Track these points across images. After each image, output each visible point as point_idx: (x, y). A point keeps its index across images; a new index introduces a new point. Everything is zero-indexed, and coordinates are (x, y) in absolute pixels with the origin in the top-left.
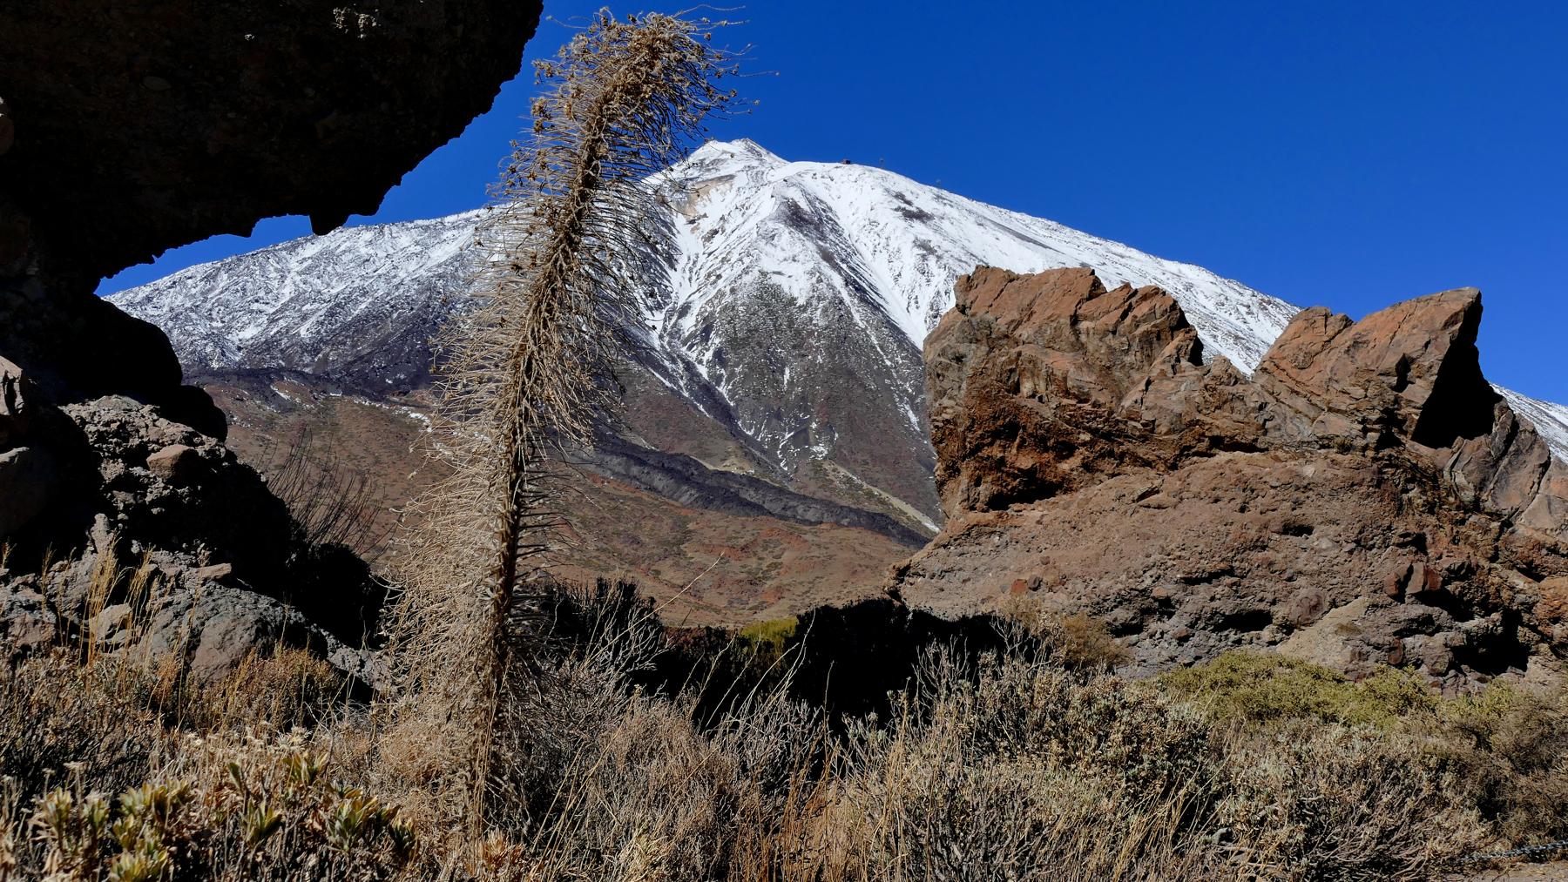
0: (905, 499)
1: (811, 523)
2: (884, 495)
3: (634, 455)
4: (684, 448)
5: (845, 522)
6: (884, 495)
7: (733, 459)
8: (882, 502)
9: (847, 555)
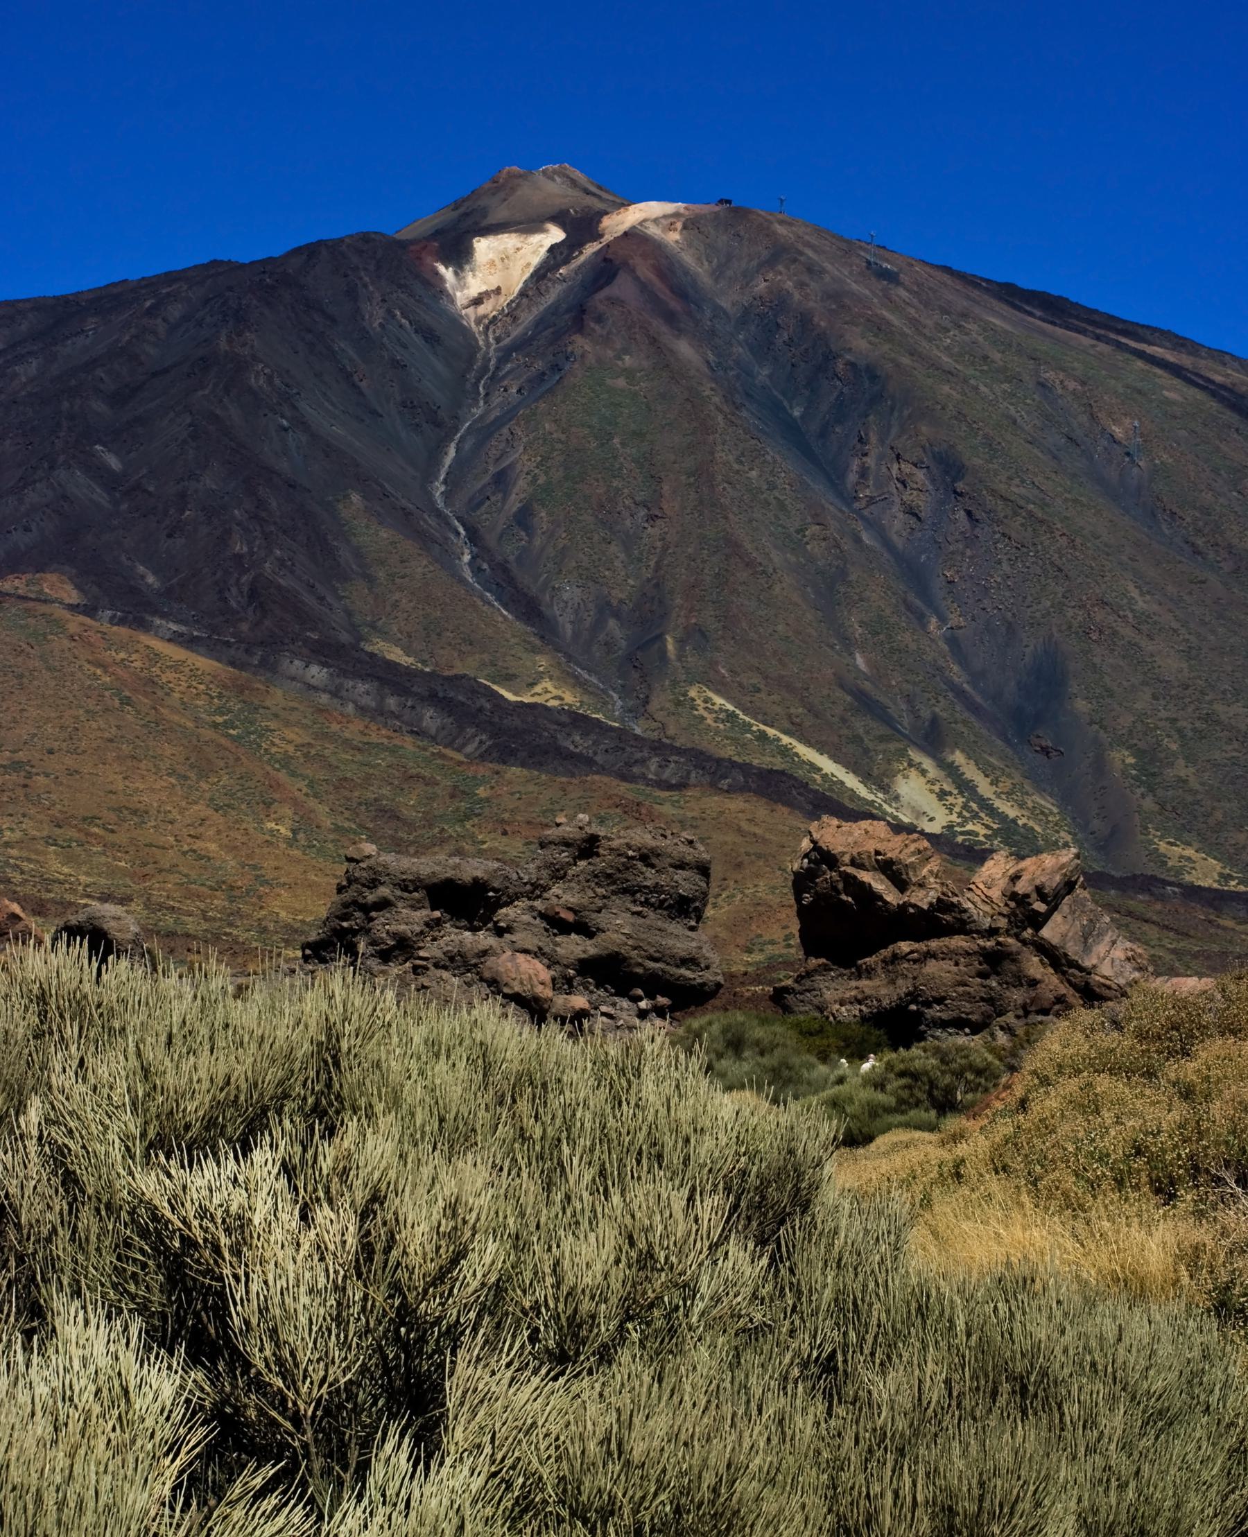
0: (821, 748)
3: (389, 677)
4: (465, 667)
5: (724, 784)
6: (786, 740)
7: (547, 684)
8: (785, 752)
9: (731, 838)
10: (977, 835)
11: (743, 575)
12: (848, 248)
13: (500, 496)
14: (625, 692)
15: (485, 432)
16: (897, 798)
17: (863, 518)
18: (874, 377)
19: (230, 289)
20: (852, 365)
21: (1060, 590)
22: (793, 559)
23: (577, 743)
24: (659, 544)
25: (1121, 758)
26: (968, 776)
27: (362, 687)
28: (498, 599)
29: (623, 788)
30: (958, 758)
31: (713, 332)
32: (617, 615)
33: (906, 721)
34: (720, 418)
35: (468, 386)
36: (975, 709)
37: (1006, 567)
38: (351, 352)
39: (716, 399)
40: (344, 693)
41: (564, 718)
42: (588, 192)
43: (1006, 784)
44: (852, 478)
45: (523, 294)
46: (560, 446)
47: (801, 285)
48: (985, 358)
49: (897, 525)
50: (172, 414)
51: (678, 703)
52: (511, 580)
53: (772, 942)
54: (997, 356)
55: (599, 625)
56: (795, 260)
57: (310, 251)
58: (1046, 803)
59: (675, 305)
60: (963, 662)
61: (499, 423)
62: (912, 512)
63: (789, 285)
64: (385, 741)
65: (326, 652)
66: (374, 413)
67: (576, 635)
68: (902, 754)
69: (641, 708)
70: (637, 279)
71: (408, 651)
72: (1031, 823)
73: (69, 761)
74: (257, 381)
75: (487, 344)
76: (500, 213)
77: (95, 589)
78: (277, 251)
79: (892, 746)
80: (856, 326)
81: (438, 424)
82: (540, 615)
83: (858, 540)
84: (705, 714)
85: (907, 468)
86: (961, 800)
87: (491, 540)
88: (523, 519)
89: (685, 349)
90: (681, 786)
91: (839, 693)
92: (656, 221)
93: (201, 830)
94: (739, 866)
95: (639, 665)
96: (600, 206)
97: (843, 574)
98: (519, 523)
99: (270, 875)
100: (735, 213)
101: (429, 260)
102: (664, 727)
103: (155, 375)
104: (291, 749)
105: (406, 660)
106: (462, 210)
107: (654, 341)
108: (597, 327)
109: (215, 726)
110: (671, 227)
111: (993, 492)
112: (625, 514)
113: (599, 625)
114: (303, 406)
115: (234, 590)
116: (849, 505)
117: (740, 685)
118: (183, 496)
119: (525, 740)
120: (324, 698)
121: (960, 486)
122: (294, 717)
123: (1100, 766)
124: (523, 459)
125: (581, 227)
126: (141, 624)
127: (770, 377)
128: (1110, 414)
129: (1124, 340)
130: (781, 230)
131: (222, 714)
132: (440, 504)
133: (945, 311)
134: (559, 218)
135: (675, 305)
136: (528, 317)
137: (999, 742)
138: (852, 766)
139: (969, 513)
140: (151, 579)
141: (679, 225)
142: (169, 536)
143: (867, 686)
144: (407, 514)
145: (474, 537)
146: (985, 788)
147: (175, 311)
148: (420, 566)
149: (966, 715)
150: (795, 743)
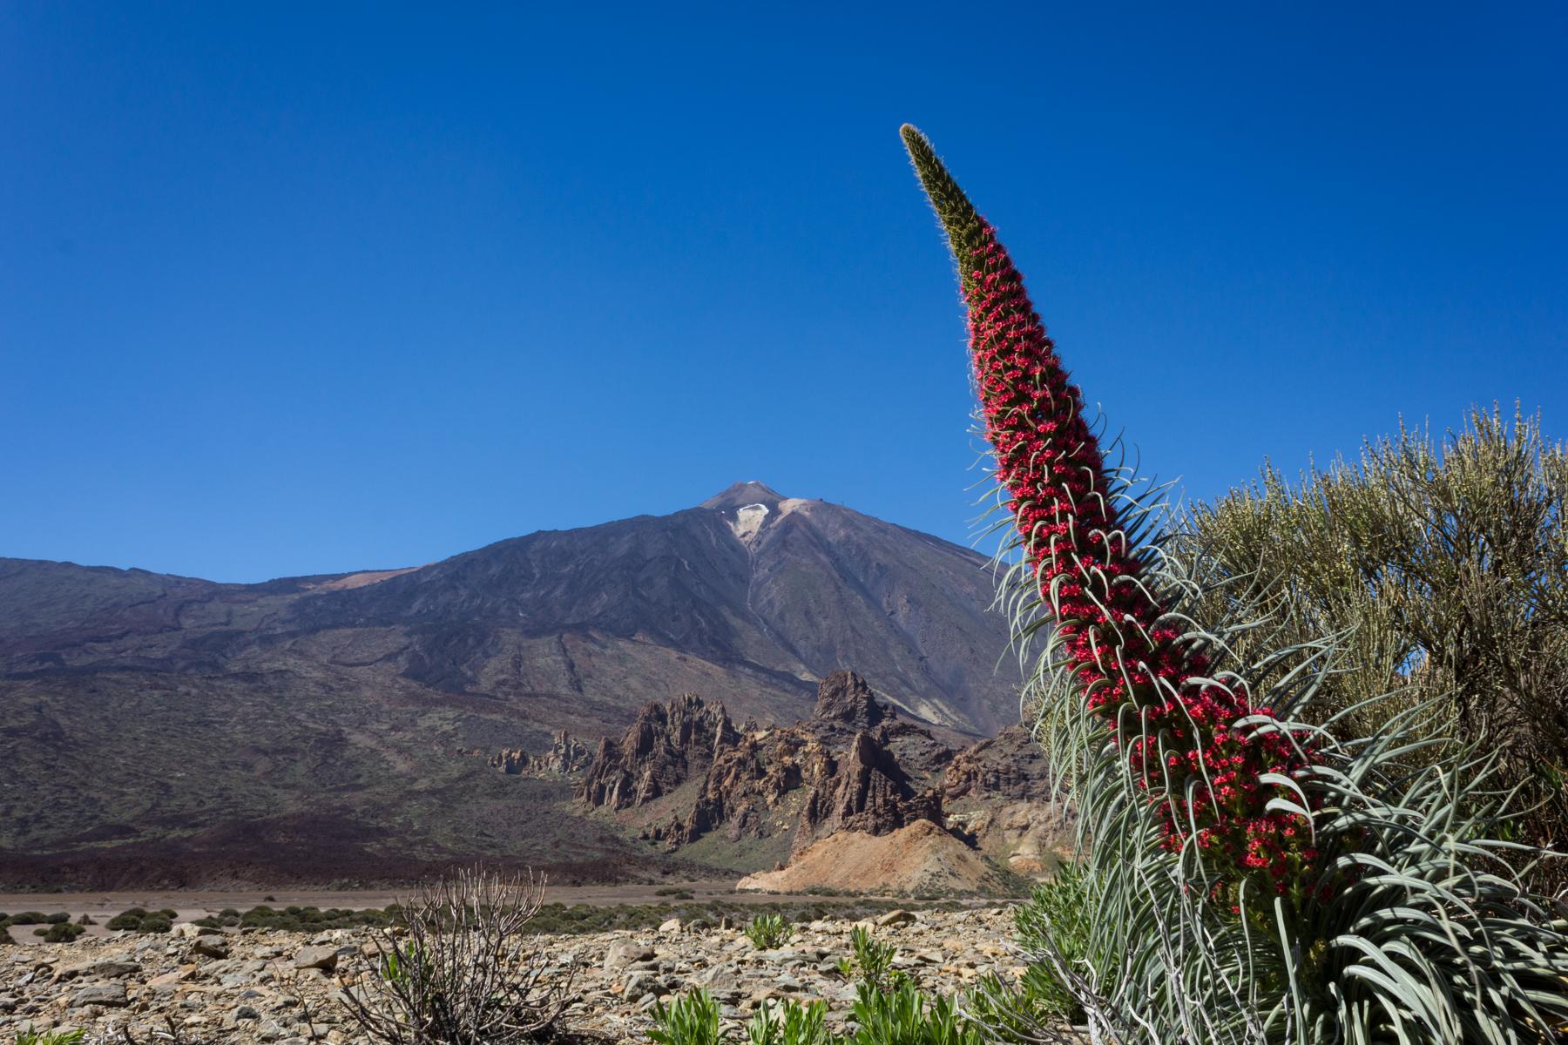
12: (869, 519)
15: (759, 584)
25: (986, 702)
76: (740, 501)
88: (781, 616)
89: (823, 557)
123: (980, 704)
136: (764, 542)
145: (766, 622)
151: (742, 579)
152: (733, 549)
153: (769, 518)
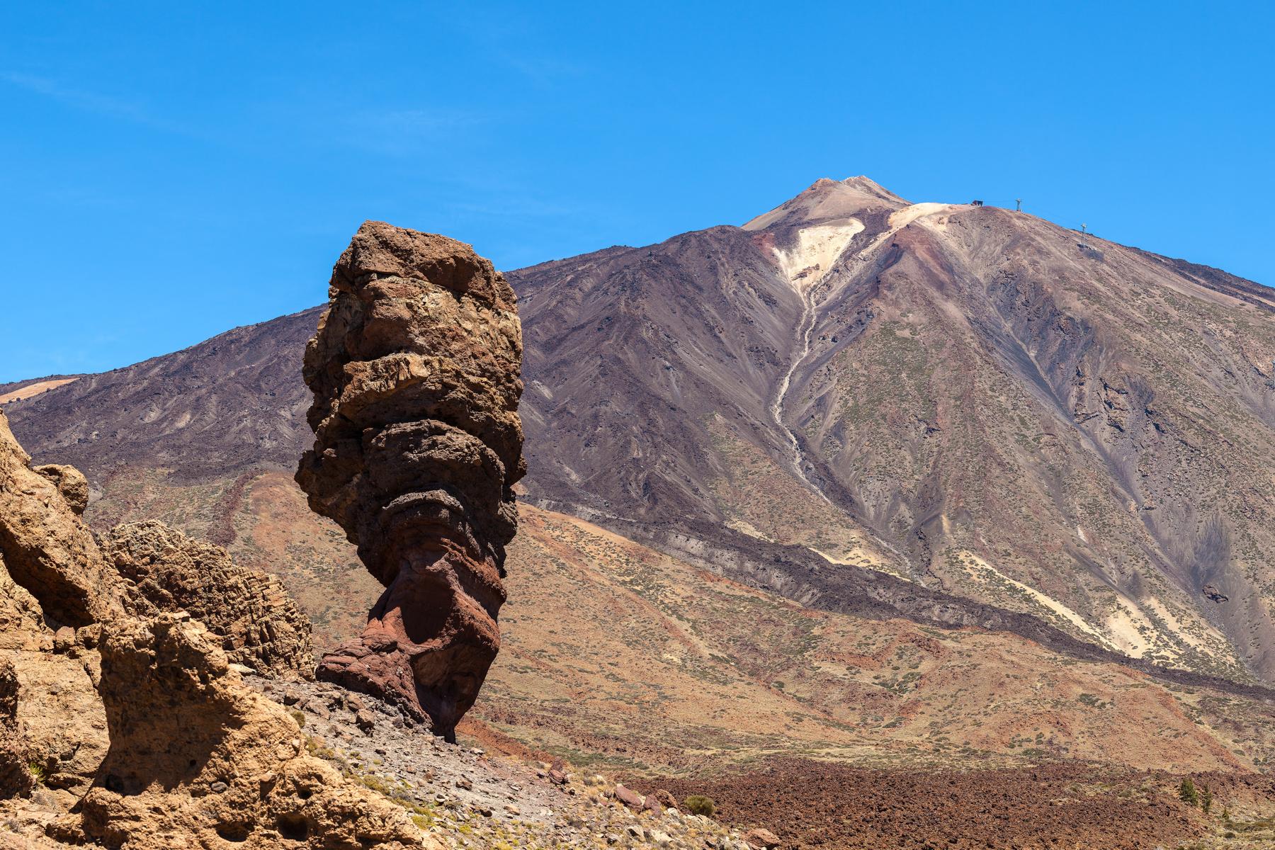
0: (1054, 595)
1: (949, 627)
2: (1029, 591)
3: (744, 546)
4: (801, 538)
5: (988, 624)
6: (1029, 591)
8: (1028, 599)
10: (1168, 658)
11: (997, 471)
13: (821, 415)
14: (912, 555)
15: (809, 369)
16: (1110, 632)
17: (1081, 429)
18: (1087, 328)
19: (627, 267)
20: (1070, 318)
21: (1223, 481)
22: (1032, 460)
23: (880, 594)
24: (935, 449)
26: (1160, 616)
27: (727, 555)
28: (822, 490)
29: (916, 629)
30: (1153, 602)
31: (971, 297)
32: (906, 500)
33: (1115, 576)
34: (978, 358)
35: (798, 336)
36: (1165, 568)
37: (1184, 463)
38: (713, 312)
39: (974, 345)
40: (714, 559)
41: (871, 576)
42: (880, 197)
43: (1187, 622)
44: (1073, 401)
45: (836, 270)
46: (862, 379)
47: (1034, 263)
48: (1166, 314)
49: (1106, 435)
50: (587, 358)
51: (952, 564)
52: (830, 475)
53: (1029, 740)
54: (1174, 313)
55: (893, 508)
56: (1029, 245)
57: (683, 240)
58: (1217, 634)
59: (944, 277)
60: (1156, 534)
61: (819, 363)
62: (1116, 425)
63: (1025, 262)
64: (746, 594)
65: (701, 528)
66: (730, 355)
67: (878, 516)
68: (1111, 600)
69: (925, 567)
70: (916, 258)
71: (757, 527)
72: (1206, 650)
73: (523, 611)
74: (646, 334)
75: (811, 308)
76: (817, 212)
77: (535, 484)
78: (660, 239)
79: (1107, 594)
80: (1073, 290)
81: (775, 363)
82: (851, 501)
83: (1078, 446)
84: (971, 572)
85: (1112, 394)
86: (1156, 633)
87: (815, 447)
88: (838, 431)
89: (952, 310)
90: (958, 626)
91: (1066, 556)
92: (929, 216)
93: (617, 660)
94: (1002, 684)
95: (921, 537)
96: (887, 205)
97: (1068, 470)
98: (835, 435)
99: (669, 693)
100: (985, 213)
101: (767, 245)
102: (942, 582)
103: (574, 329)
104: (679, 600)
105: (757, 534)
106: (790, 209)
107: (930, 303)
108: (889, 294)
109: (624, 583)
110: (940, 222)
111: (1173, 411)
112: (911, 427)
113: (893, 508)
114: (679, 350)
115: (634, 485)
116: (1071, 421)
117: (996, 551)
118: (596, 416)
119: (845, 593)
120: (701, 563)
121: (1150, 406)
122: (680, 577)
123: (1254, 607)
124: (836, 390)
125: (876, 221)
126: (568, 510)
127: (1013, 328)
128: (1256, 354)
129: (1264, 301)
130: (1018, 223)
131: (629, 575)
132: (779, 421)
133: (1136, 280)
134: (859, 214)
135: (944, 277)
136: (839, 287)
137: (1182, 591)
138: (1078, 610)
139: (1157, 427)
140: (574, 476)
141: (946, 220)
142: (587, 445)
143: (1087, 551)
144: (755, 428)
145: (803, 445)
146: (1172, 624)
147: (588, 284)
148: (765, 466)
149: (1158, 571)
150: (1036, 593)
151: (773, 361)
152: (770, 301)
153: (859, 242)
